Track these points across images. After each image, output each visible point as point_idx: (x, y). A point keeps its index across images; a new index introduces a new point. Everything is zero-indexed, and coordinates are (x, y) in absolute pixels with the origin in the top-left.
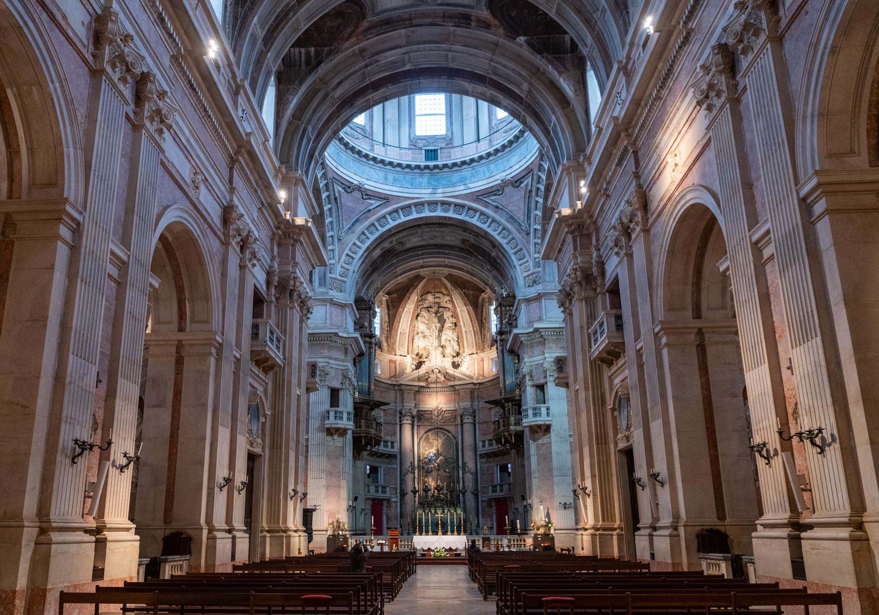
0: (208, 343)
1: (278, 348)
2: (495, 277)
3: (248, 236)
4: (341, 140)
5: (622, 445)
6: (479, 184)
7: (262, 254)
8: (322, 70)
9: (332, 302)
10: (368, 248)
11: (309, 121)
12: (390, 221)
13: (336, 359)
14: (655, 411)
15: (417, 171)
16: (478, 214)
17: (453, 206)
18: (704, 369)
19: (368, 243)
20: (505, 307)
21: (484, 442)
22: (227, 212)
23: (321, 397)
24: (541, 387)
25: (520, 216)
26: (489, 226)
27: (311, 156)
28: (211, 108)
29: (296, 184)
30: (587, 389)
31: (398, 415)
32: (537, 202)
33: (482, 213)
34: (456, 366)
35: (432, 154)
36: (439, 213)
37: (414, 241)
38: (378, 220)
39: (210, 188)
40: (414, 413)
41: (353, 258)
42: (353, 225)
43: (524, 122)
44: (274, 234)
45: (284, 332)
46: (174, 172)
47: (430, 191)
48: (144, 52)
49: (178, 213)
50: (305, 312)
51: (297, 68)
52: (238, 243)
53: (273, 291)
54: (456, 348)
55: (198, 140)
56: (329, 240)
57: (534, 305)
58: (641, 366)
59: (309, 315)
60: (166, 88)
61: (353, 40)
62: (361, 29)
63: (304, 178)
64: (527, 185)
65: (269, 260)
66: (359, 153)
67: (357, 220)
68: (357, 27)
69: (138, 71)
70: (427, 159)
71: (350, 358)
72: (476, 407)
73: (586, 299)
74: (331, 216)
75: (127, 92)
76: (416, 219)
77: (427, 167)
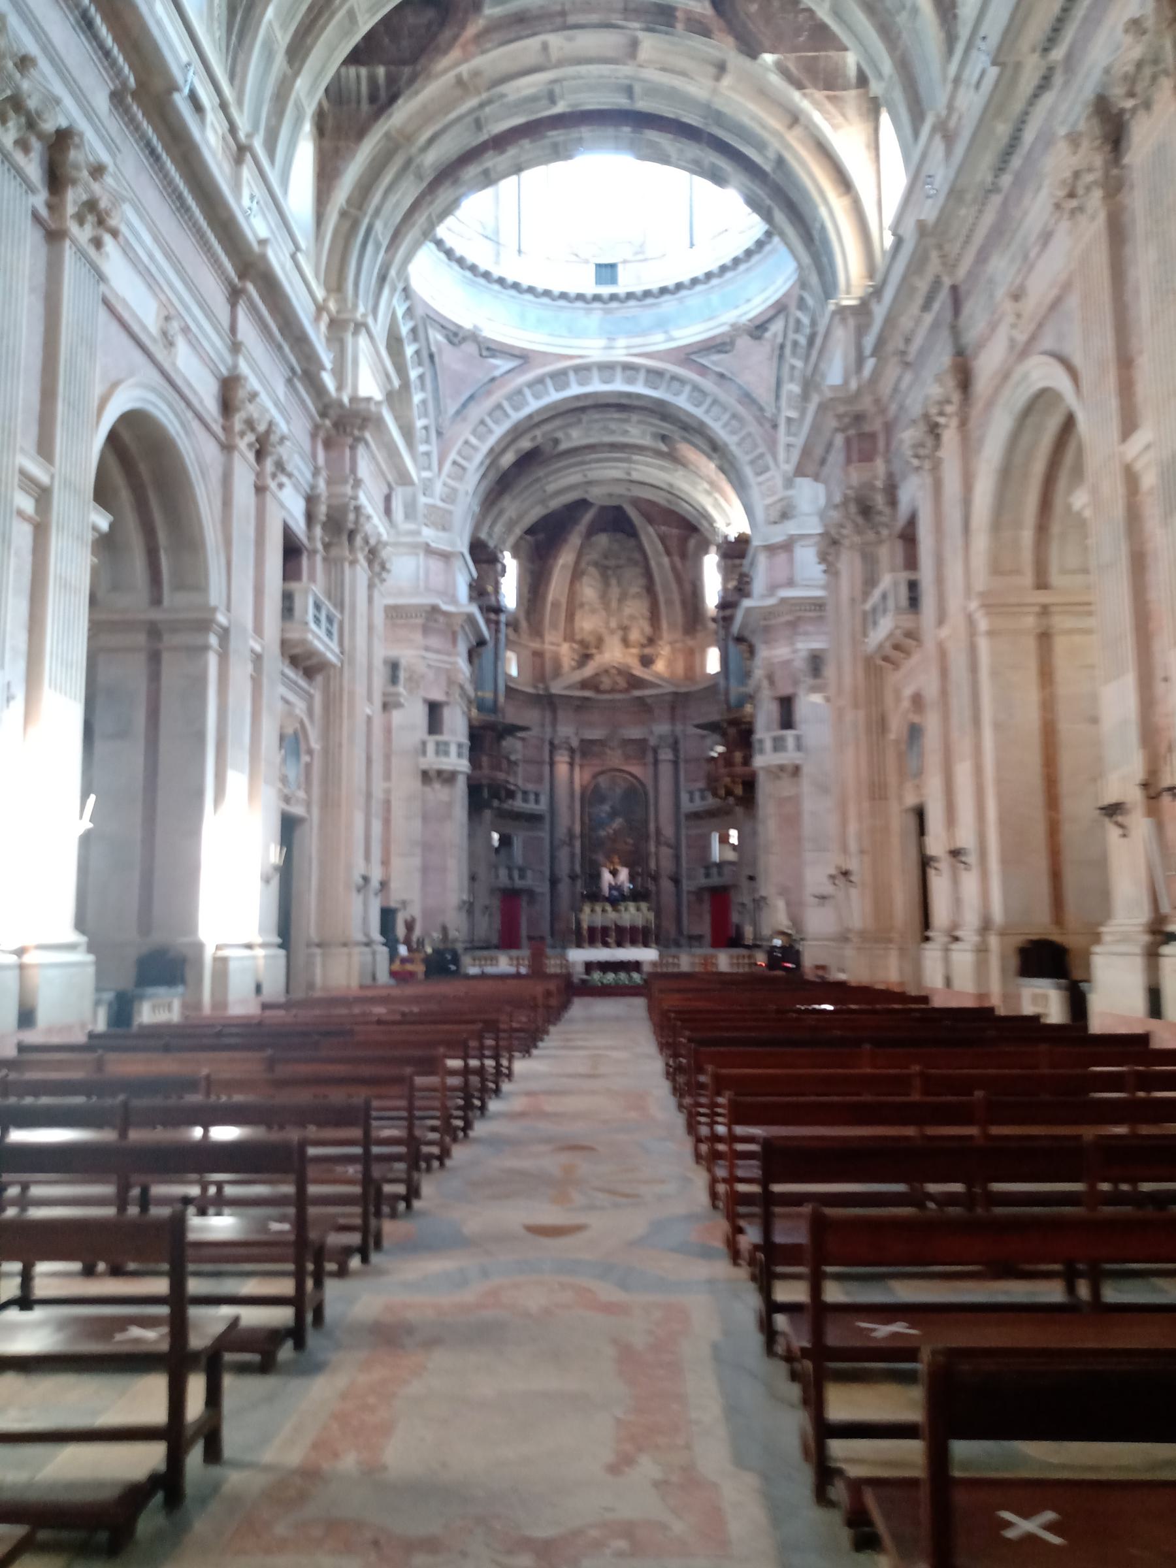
0: (204, 624)
1: (329, 633)
2: (717, 505)
3: (268, 432)
4: (439, 243)
5: (911, 800)
6: (690, 333)
7: (298, 465)
8: (401, 114)
9: (429, 551)
10: (492, 450)
11: (377, 212)
12: (530, 398)
13: (438, 652)
14: (963, 745)
16: (688, 388)
18: (1046, 675)
19: (491, 441)
21: (691, 793)
22: (229, 392)
23: (413, 715)
24: (786, 704)
25: (763, 394)
26: (707, 412)
27: (383, 278)
28: (191, 191)
29: (356, 333)
31: (547, 748)
32: (793, 367)
33: (696, 388)
34: (647, 661)
35: (607, 272)
37: (576, 437)
38: (509, 398)
39: (194, 344)
40: (575, 743)
41: (464, 469)
42: (464, 405)
43: (767, 216)
44: (317, 428)
45: (340, 606)
46: (126, 316)
47: (602, 342)
48: (59, 89)
49: (139, 393)
50: (377, 568)
51: (354, 105)
52: (250, 446)
53: (318, 531)
54: (648, 630)
55: (169, 255)
56: (420, 434)
57: (782, 557)
58: (944, 673)
59: (384, 575)
60: (105, 157)
61: (455, 53)
62: (471, 30)
63: (370, 320)
64: (775, 335)
65: (309, 475)
66: (473, 269)
67: (471, 398)
69: (49, 126)
70: (599, 281)
71: (462, 648)
74: (423, 388)
75: (33, 168)
76: (577, 398)
77: (597, 298)
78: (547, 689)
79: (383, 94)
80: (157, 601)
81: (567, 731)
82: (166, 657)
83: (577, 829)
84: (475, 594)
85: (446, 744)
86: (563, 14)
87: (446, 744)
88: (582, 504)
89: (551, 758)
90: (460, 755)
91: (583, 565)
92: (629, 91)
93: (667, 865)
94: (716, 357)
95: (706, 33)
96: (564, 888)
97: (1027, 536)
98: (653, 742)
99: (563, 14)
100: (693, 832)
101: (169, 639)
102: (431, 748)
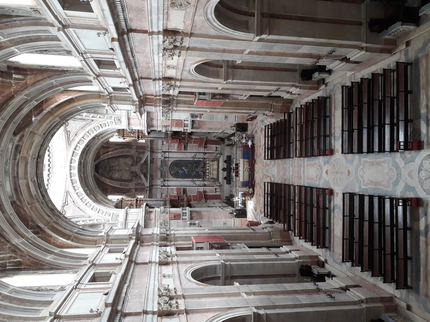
2: (102, 138)
13: (155, 216)
15: (50, 175)
16: (78, 145)
17: (73, 158)
19: (91, 202)
20: (124, 134)
30: (216, 108)
31: (163, 187)
33: (78, 143)
36: (76, 165)
42: (81, 210)
57: (132, 121)
68: (20, 206)
72: (161, 151)
73: (177, 104)
78: (147, 187)
79: (37, 230)
80: (219, 278)
81: (159, 182)
82: (232, 275)
83: (191, 179)
84: (132, 207)
85: (183, 213)
86: (15, 177)
87: (183, 213)
88: (95, 176)
89: (166, 186)
90: (185, 210)
91: (108, 177)
92: (34, 158)
93: (201, 156)
94: (71, 136)
95: (22, 136)
96: (206, 183)
97: (211, 69)
98: (163, 158)
99: (14, 177)
100: (188, 149)
101: (228, 274)
102: (184, 217)
